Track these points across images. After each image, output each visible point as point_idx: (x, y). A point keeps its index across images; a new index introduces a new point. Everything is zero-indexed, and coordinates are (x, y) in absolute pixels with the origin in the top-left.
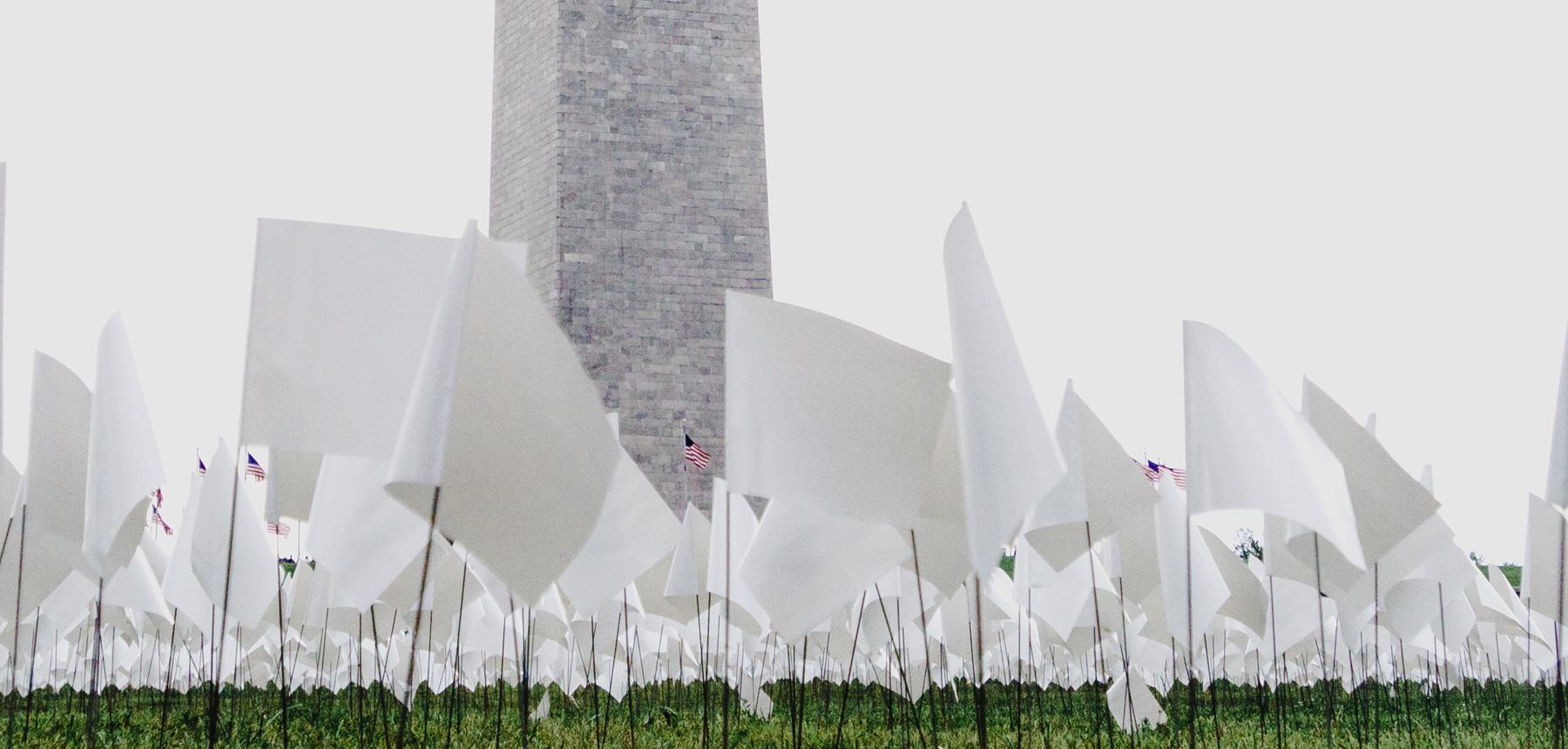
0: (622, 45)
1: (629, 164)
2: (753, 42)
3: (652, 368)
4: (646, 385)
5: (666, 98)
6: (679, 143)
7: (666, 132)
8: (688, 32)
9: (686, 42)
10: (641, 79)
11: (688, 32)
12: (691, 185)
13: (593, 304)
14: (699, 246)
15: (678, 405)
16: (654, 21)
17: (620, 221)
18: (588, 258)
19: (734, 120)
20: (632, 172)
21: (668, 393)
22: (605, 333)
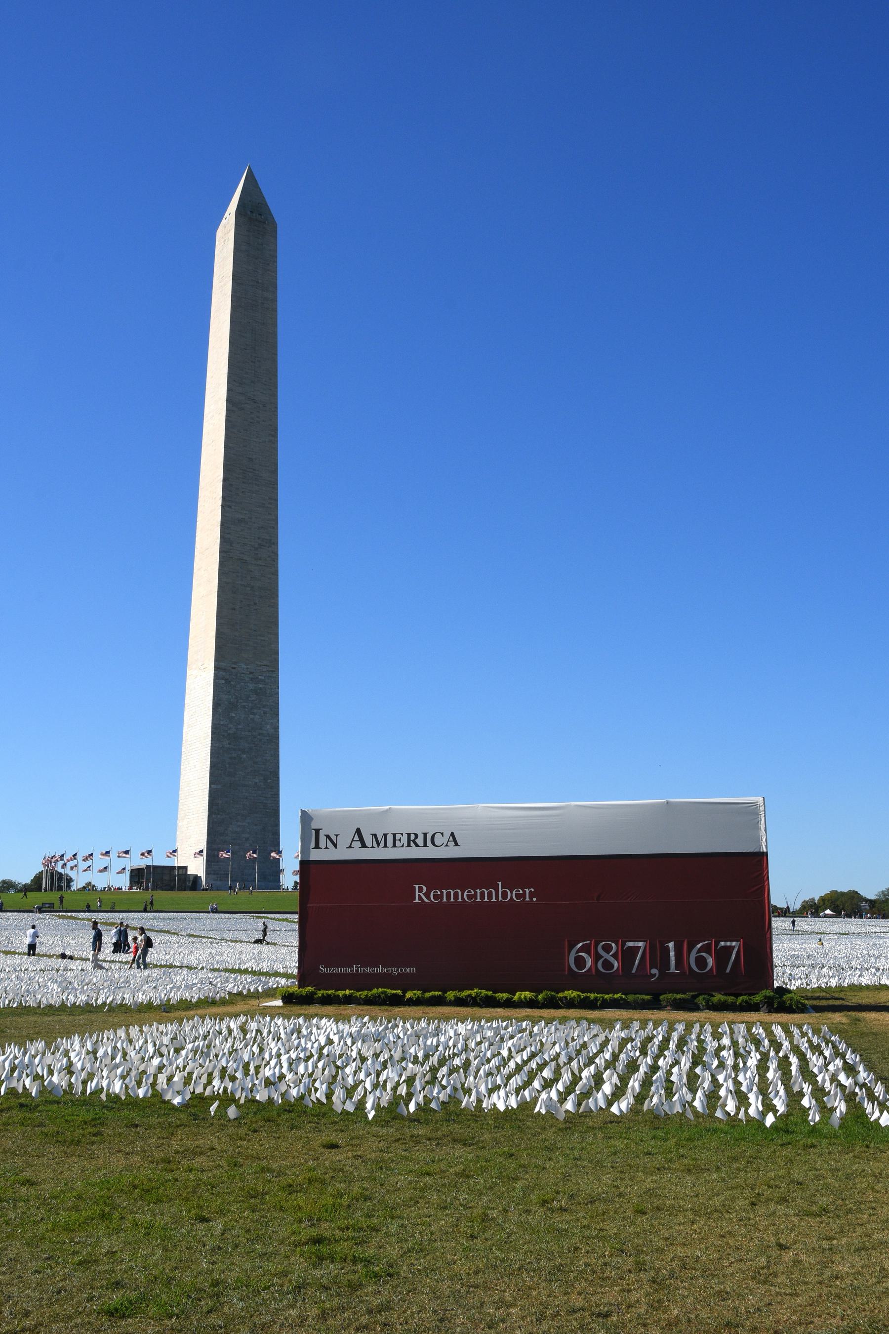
0: (233, 715)
1: (234, 755)
2: (277, 715)
3: (239, 823)
5: (247, 733)
8: (255, 711)
9: (254, 714)
10: (239, 727)
11: (255, 711)
13: (220, 802)
14: (256, 783)
15: (247, 836)
16: (244, 707)
18: (219, 787)
20: (235, 758)
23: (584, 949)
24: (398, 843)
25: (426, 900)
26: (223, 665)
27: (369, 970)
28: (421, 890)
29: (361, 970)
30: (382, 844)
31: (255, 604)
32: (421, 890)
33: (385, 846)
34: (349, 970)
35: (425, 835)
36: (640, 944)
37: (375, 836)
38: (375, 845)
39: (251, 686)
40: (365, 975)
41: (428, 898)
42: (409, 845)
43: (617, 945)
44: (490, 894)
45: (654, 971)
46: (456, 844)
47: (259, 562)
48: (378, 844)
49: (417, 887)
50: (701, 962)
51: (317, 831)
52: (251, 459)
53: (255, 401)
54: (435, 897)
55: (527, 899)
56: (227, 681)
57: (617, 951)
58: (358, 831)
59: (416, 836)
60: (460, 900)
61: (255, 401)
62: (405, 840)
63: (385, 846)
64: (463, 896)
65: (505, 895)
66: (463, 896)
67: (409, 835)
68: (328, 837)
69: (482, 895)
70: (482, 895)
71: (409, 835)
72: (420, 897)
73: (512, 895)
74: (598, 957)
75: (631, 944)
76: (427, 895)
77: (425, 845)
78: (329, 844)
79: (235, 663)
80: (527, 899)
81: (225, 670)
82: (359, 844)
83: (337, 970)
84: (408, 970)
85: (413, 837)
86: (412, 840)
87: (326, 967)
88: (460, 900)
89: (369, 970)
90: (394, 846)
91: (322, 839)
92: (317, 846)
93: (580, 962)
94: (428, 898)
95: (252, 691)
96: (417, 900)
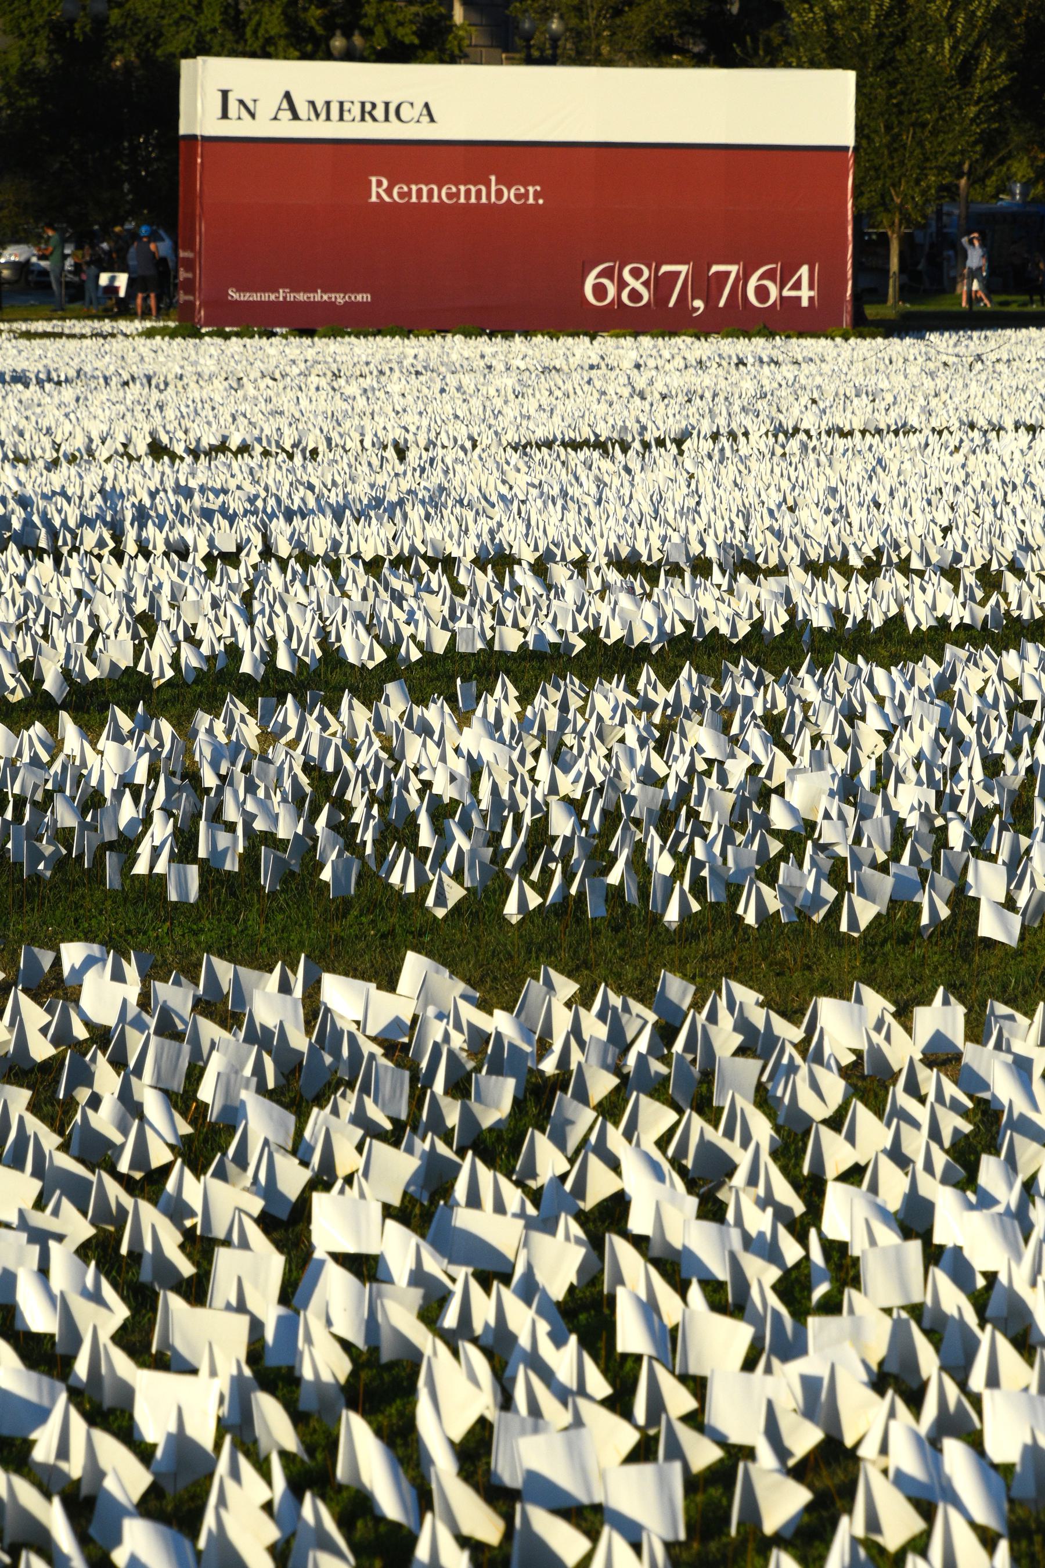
23: (607, 273)
24: (346, 115)
25: (387, 199)
27: (302, 297)
28: (379, 184)
29: (291, 297)
30: (323, 116)
32: (379, 184)
33: (328, 118)
34: (273, 297)
35: (387, 104)
36: (683, 269)
37: (312, 103)
38: (313, 116)
40: (296, 304)
41: (390, 195)
42: (363, 119)
43: (649, 268)
44: (479, 193)
45: (698, 304)
46: (432, 120)
48: (317, 115)
49: (374, 179)
50: (762, 293)
51: (225, 94)
54: (401, 195)
55: (531, 201)
57: (648, 280)
58: (287, 96)
59: (374, 106)
60: (436, 200)
62: (356, 111)
63: (328, 118)
64: (441, 194)
65: (499, 194)
66: (441, 194)
67: (363, 104)
68: (241, 102)
69: (468, 194)
70: (468, 194)
71: (363, 104)
72: (378, 195)
73: (510, 195)
74: (622, 284)
75: (665, 268)
76: (389, 191)
77: (387, 119)
78: (244, 113)
80: (531, 201)
82: (288, 114)
83: (256, 297)
84: (359, 298)
85: (368, 107)
86: (367, 112)
87: (239, 290)
88: (436, 200)
89: (302, 297)
90: (341, 119)
91: (233, 107)
92: (225, 115)
93: (600, 291)
94: (390, 195)
96: (374, 199)
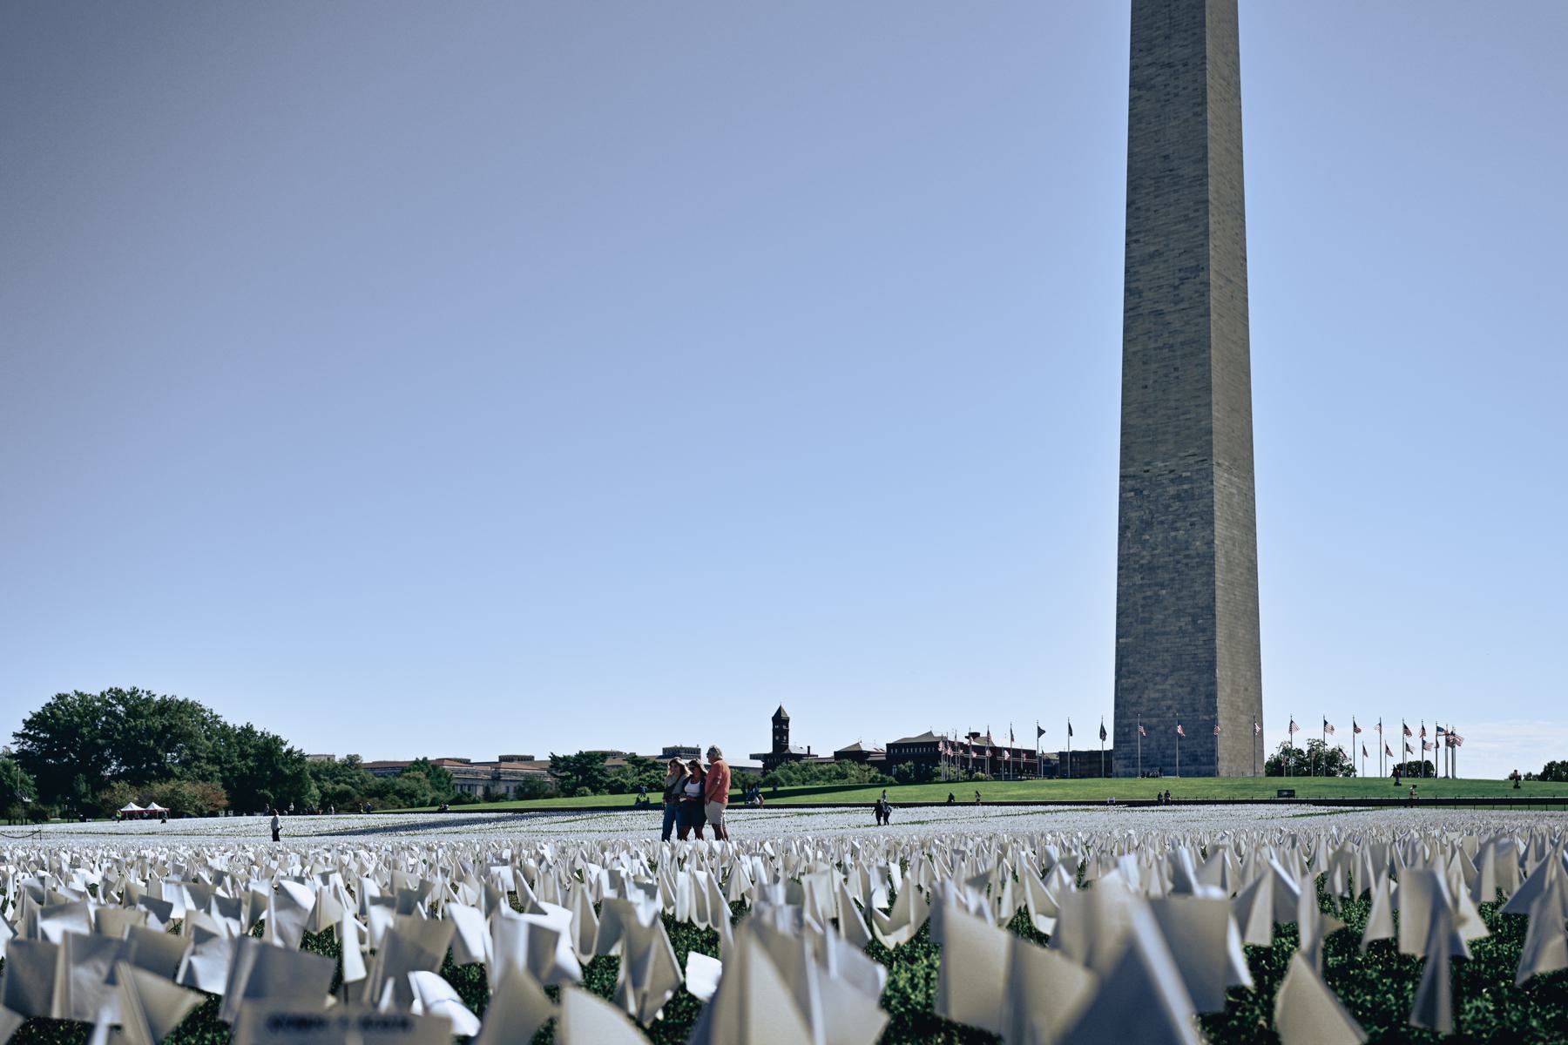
4: (1153, 695)
6: (1173, 579)
7: (1167, 576)
9: (1177, 530)
12: (1178, 599)
16: (1162, 523)
17: (1143, 621)
19: (1200, 564)
21: (1164, 698)
22: (1137, 673)
26: (1131, 470)
31: (1176, 369)
39: (1172, 490)
47: (1182, 306)
52: (1167, 157)
53: (1170, 65)
56: (1138, 492)
61: (1170, 65)
79: (1148, 464)
81: (1134, 477)
95: (1172, 497)
